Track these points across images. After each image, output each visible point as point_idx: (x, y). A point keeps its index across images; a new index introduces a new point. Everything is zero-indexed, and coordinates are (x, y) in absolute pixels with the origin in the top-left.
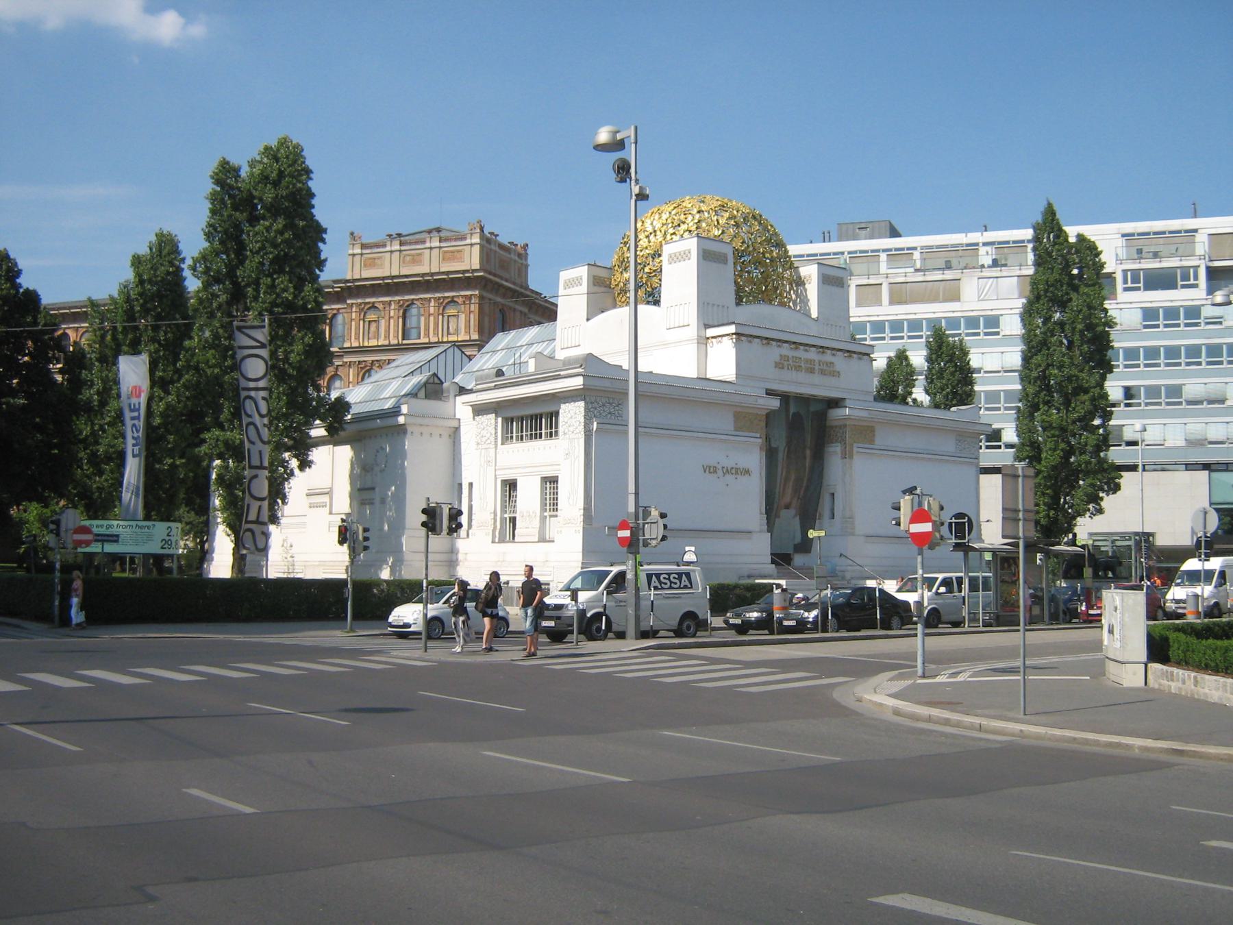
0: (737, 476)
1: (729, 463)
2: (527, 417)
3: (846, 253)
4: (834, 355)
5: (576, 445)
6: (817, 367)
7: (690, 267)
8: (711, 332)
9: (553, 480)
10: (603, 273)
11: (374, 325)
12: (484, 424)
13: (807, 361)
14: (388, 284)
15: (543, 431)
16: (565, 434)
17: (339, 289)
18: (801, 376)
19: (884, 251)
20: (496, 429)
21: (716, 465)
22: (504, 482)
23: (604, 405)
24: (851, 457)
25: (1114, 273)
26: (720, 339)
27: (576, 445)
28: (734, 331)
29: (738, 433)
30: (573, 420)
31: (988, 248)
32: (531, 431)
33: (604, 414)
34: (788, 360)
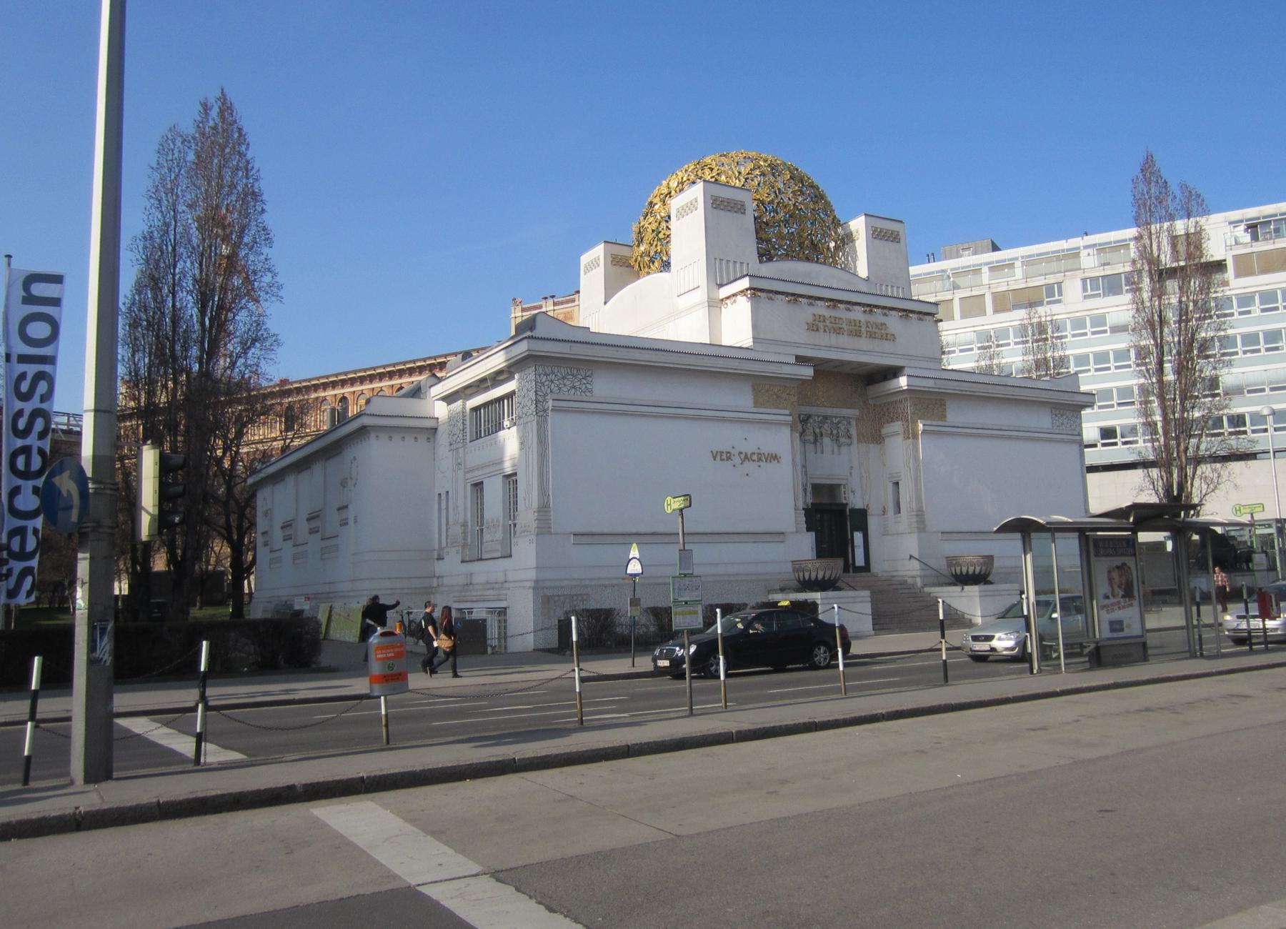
0: (761, 463)
1: (749, 448)
3: (949, 270)
4: (885, 315)
6: (863, 329)
7: (697, 219)
8: (725, 292)
13: (850, 322)
18: (844, 340)
19: (986, 264)
25: (1225, 260)
26: (734, 299)
28: (747, 285)
30: (526, 399)
31: (1090, 251)
33: (565, 389)
34: (824, 321)
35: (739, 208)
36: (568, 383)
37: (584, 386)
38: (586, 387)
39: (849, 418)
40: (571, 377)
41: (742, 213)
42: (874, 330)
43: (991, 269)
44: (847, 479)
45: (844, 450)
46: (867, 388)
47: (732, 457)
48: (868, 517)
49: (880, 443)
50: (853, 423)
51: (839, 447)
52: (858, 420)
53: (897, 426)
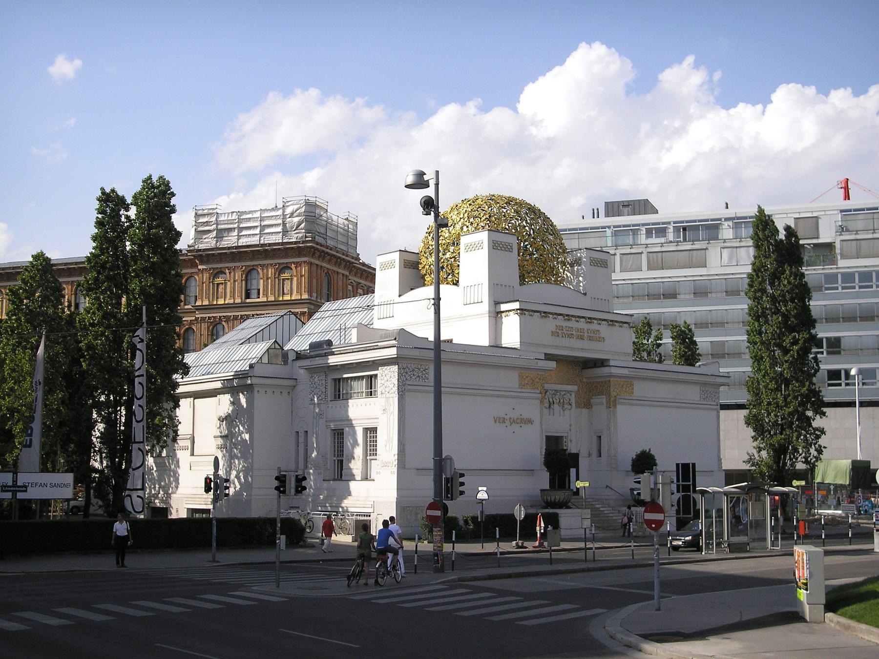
0: (522, 425)
1: (515, 415)
5: (392, 403)
6: (586, 334)
9: (374, 430)
10: (413, 258)
11: (221, 287)
13: (578, 330)
14: (233, 253)
18: (575, 343)
19: (643, 225)
23: (413, 370)
24: (615, 406)
25: (835, 243)
27: (392, 403)
28: (518, 307)
30: (389, 383)
31: (730, 223)
42: (592, 335)
43: (649, 233)
45: (567, 412)
46: (583, 370)
48: (580, 459)
50: (573, 394)
52: (576, 393)
53: (604, 399)
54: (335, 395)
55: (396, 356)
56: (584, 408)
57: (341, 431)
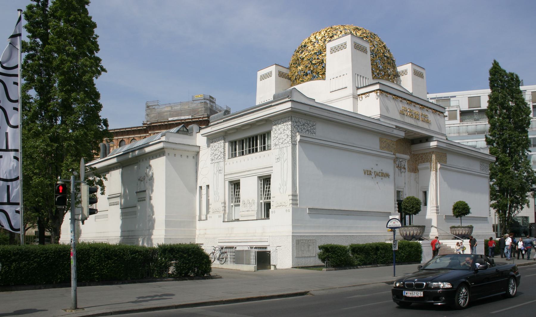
0: (383, 178)
1: (378, 169)
2: (246, 139)
5: (285, 151)
12: (216, 147)
14: (166, 124)
15: (258, 147)
16: (276, 145)
17: (145, 128)
20: (224, 149)
21: (371, 170)
22: (231, 182)
23: (304, 125)
27: (285, 151)
29: (380, 151)
30: (282, 135)
32: (250, 147)
33: (304, 131)
35: (364, 50)
36: (306, 128)
37: (312, 130)
38: (313, 131)
39: (406, 159)
40: (306, 125)
41: (366, 53)
44: (403, 189)
47: (372, 174)
49: (415, 173)
50: (407, 162)
51: (401, 173)
54: (232, 154)
55: (290, 109)
56: (412, 172)
57: (238, 182)
